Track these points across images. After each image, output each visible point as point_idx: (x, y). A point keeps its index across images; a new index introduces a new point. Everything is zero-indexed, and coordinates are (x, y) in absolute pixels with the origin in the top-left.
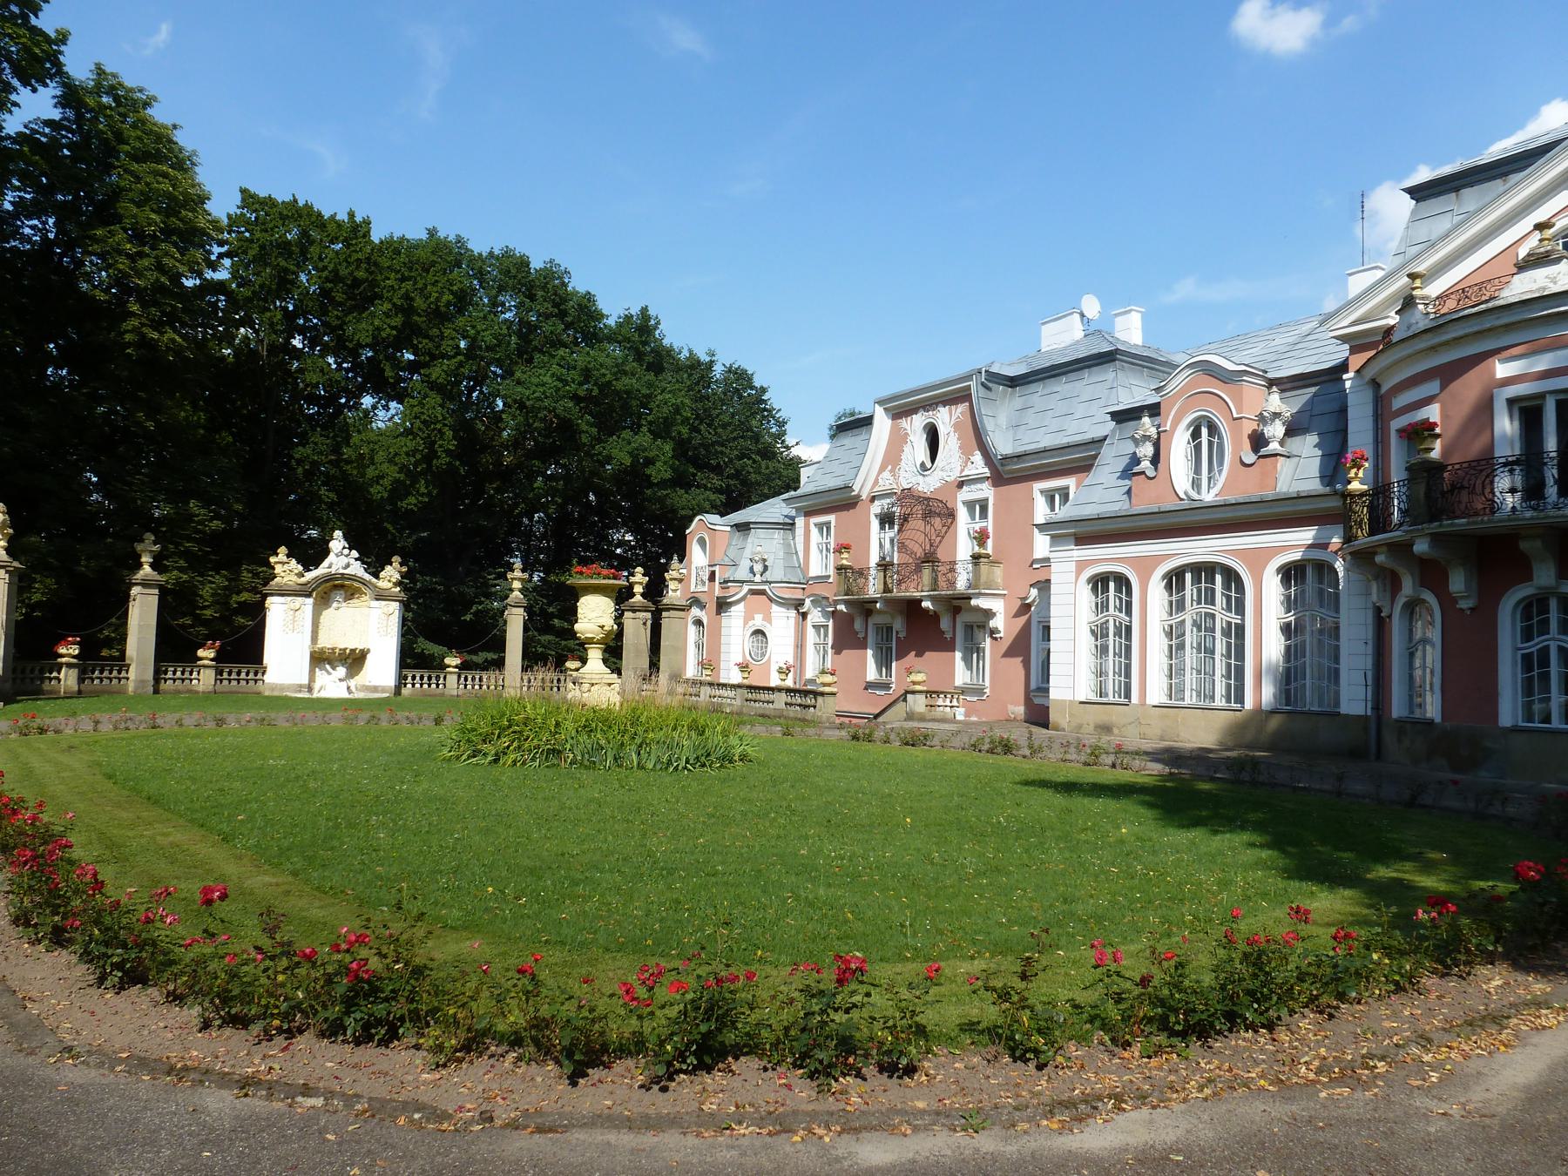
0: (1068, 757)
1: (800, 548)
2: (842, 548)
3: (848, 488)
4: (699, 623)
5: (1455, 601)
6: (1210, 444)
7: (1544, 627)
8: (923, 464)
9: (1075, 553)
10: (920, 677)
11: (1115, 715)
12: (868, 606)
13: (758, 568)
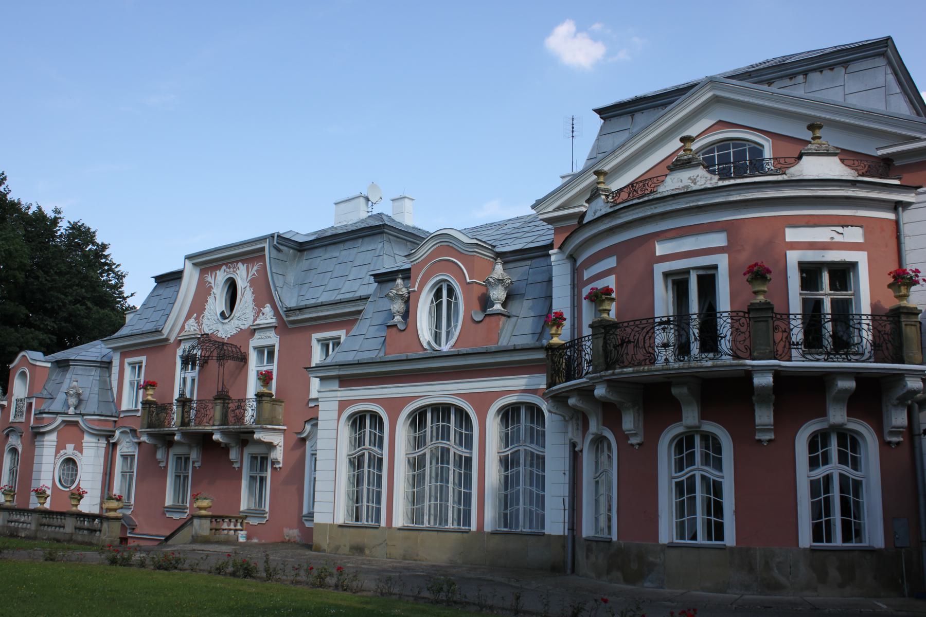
0: (299, 578)
1: (115, 384)
2: (149, 385)
3: (158, 331)
4: (14, 451)
5: (627, 437)
6: (449, 303)
7: (691, 461)
8: (222, 314)
9: (339, 394)
10: (205, 503)
11: (366, 538)
12: (168, 438)
13: (72, 401)
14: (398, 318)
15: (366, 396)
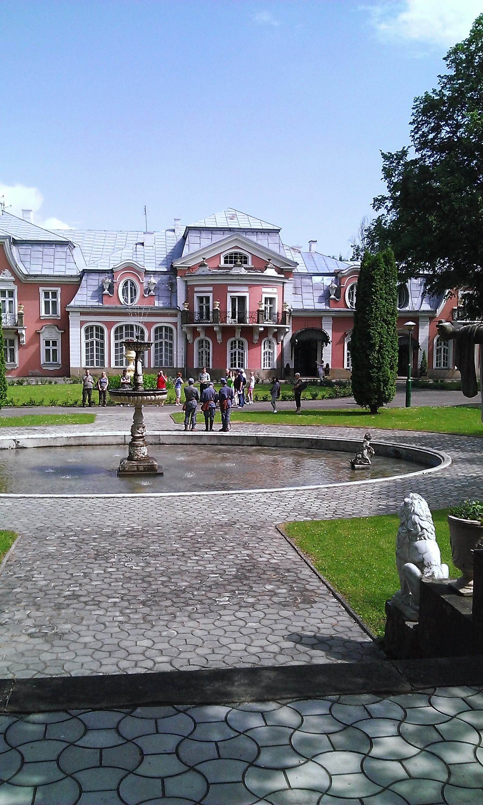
14: (106, 292)
15: (94, 320)
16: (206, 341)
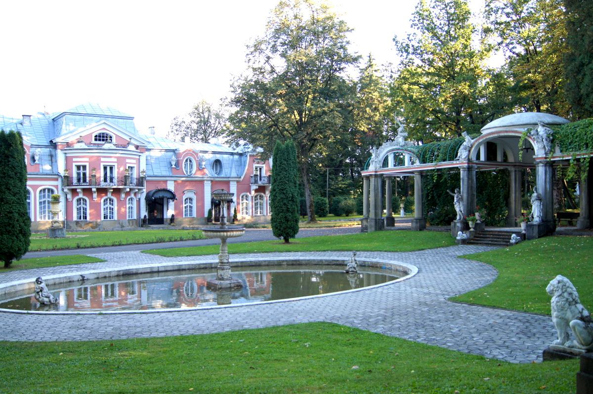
16: (83, 199)
